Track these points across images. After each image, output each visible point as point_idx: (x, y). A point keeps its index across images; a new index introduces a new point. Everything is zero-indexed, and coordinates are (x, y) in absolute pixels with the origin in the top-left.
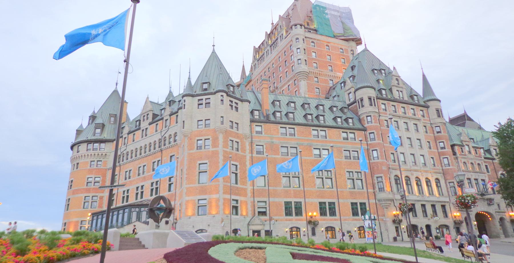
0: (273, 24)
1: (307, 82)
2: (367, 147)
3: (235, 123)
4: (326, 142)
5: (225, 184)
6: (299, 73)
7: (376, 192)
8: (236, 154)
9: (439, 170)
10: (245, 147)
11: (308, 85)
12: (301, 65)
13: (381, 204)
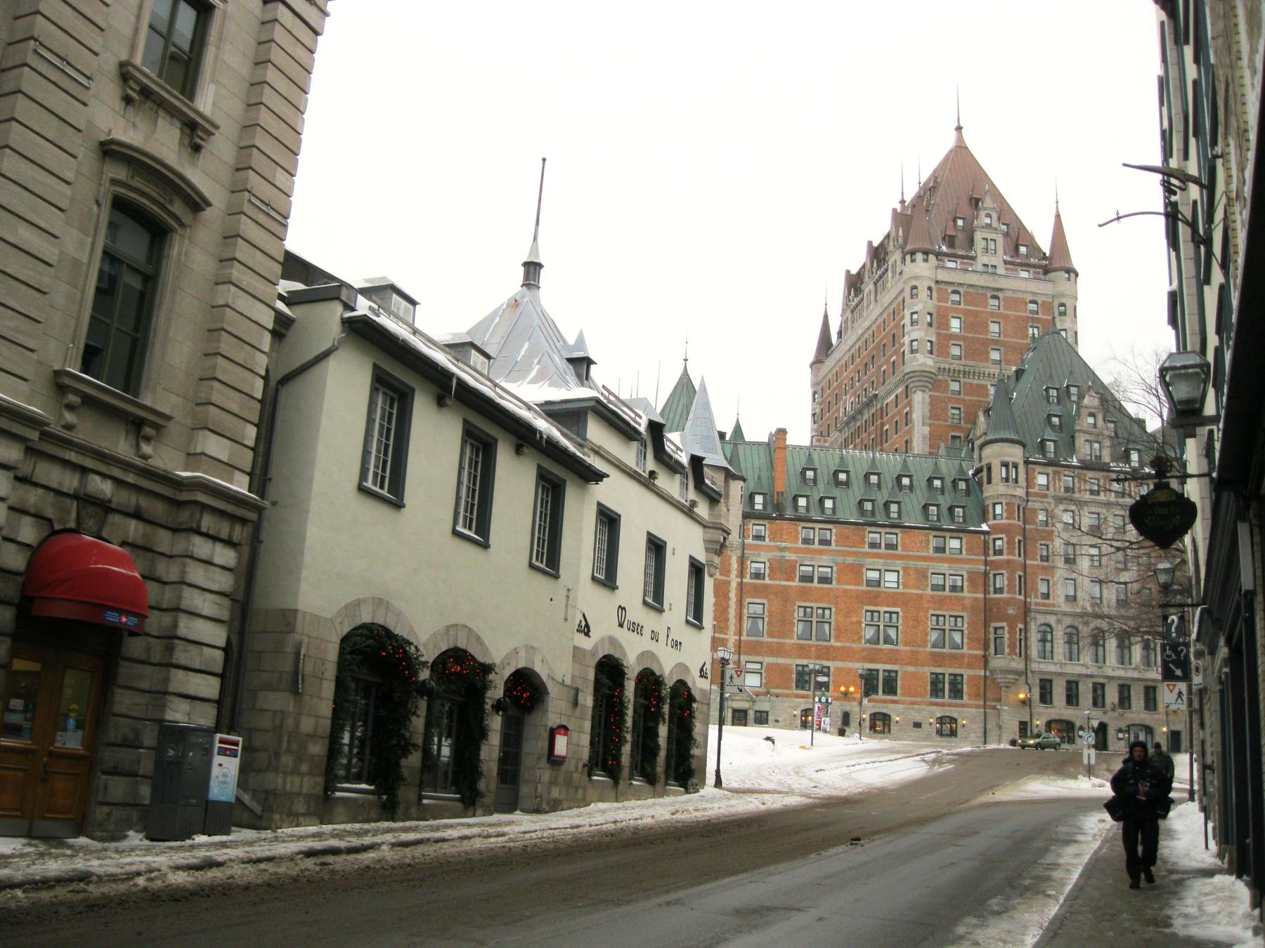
1: (930, 396)
2: (983, 568)
4: (895, 557)
12: (918, 355)
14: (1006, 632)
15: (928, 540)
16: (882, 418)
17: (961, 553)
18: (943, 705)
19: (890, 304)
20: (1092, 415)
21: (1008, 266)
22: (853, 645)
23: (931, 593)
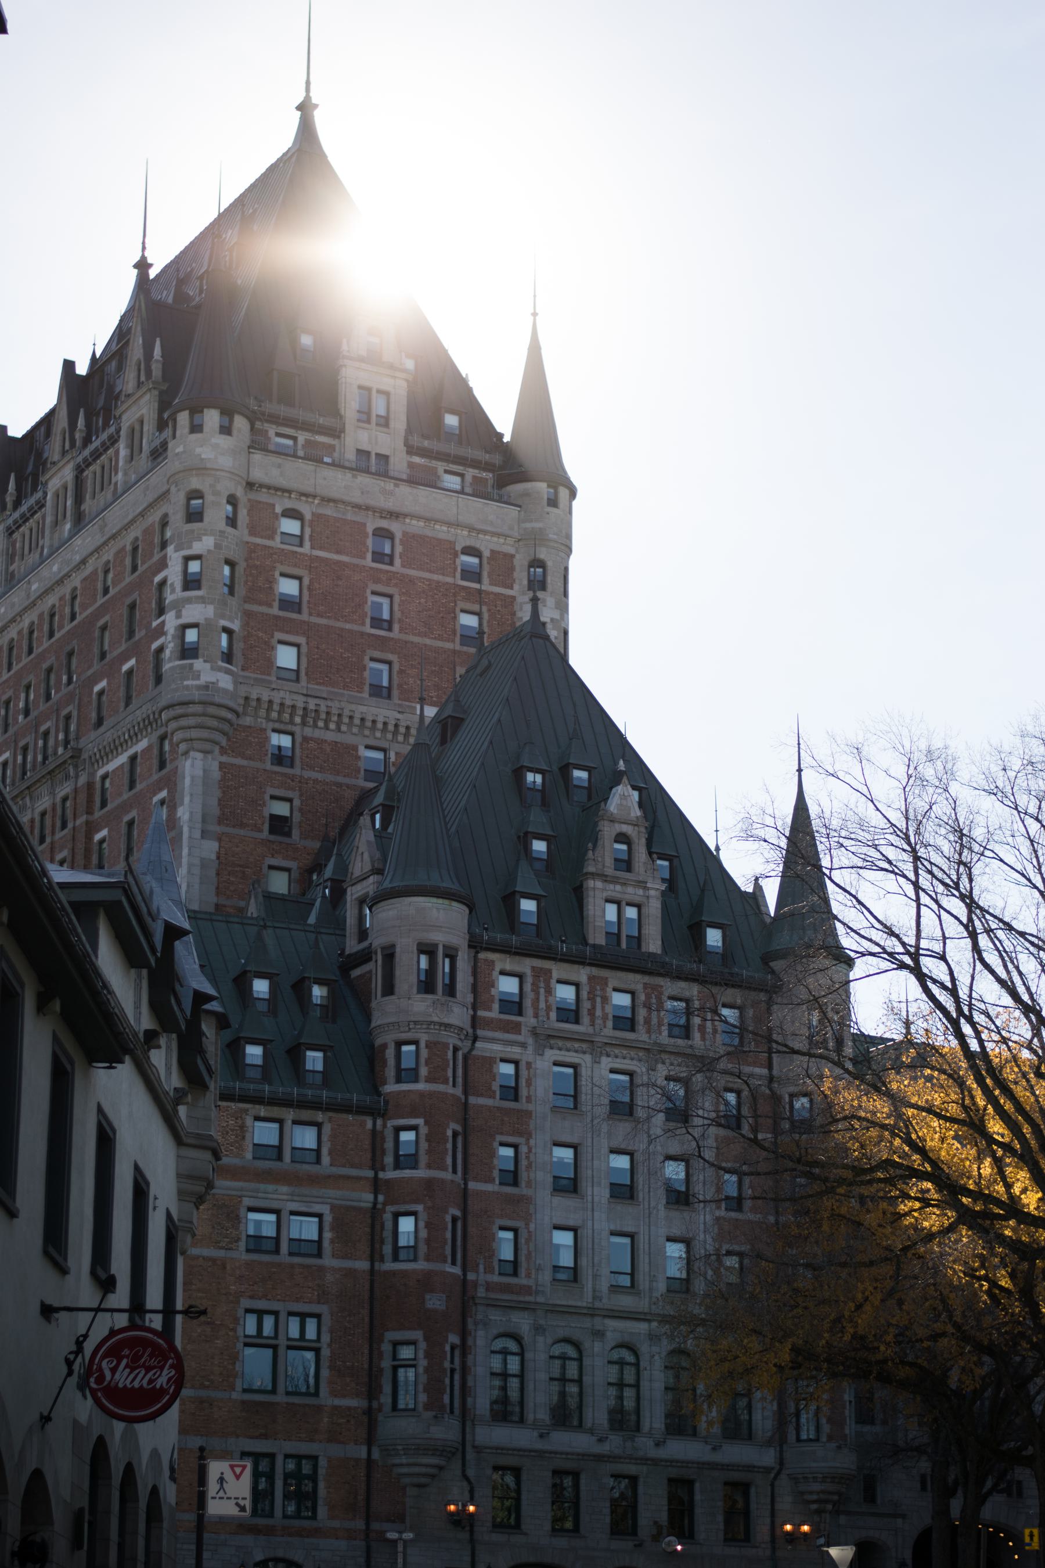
0: (142, 266)
1: (222, 766)
2: (370, 1197)
6: (179, 710)
7: (380, 1410)
11: (223, 779)
12: (198, 664)
13: (394, 1465)
14: (421, 1354)
15: (242, 1127)
16: (89, 811)
17: (318, 1161)
18: (270, 1531)
19: (126, 527)
20: (621, 838)
21: (417, 460)
23: (245, 1257)
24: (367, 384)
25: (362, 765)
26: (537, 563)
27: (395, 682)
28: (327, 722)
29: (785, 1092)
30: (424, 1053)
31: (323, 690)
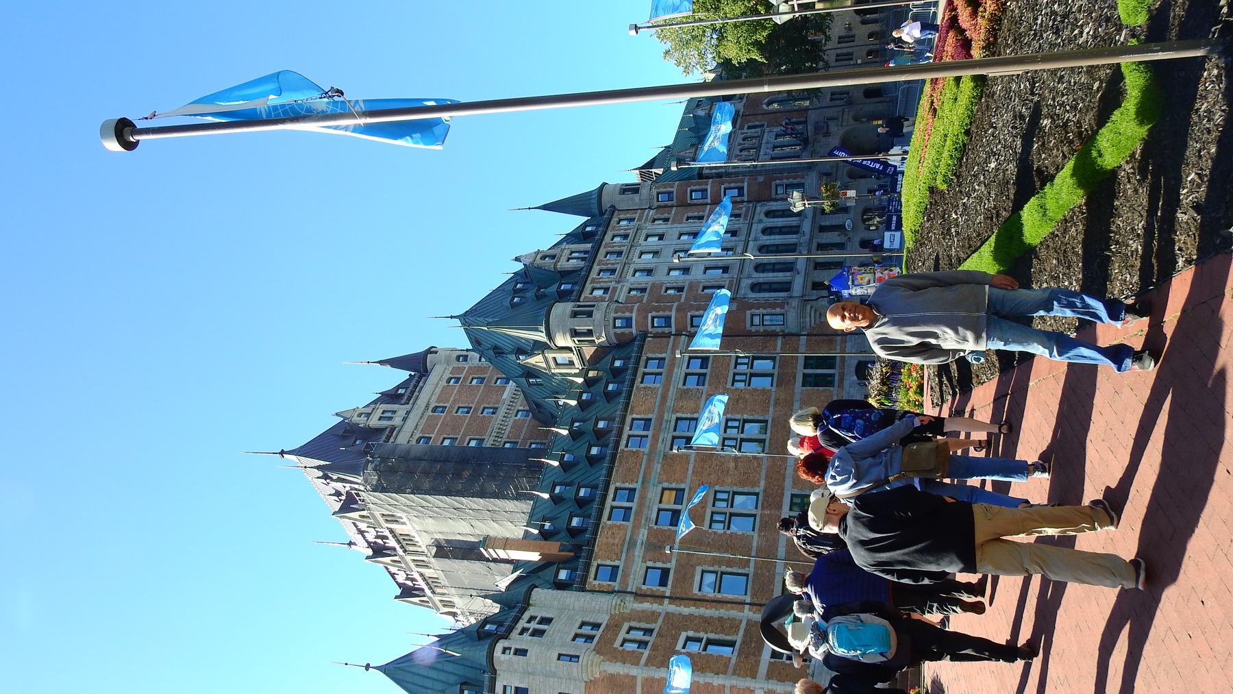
3: (580, 628)
5: (730, 670)
8: (660, 635)
9: (749, 207)
10: (643, 612)
14: (757, 312)
15: (645, 388)
18: (842, 375)
22: (764, 467)
24: (378, 417)
25: (522, 418)
26: (458, 358)
27: (492, 406)
28: (502, 429)
29: (656, 204)
30: (619, 314)
31: (490, 430)
